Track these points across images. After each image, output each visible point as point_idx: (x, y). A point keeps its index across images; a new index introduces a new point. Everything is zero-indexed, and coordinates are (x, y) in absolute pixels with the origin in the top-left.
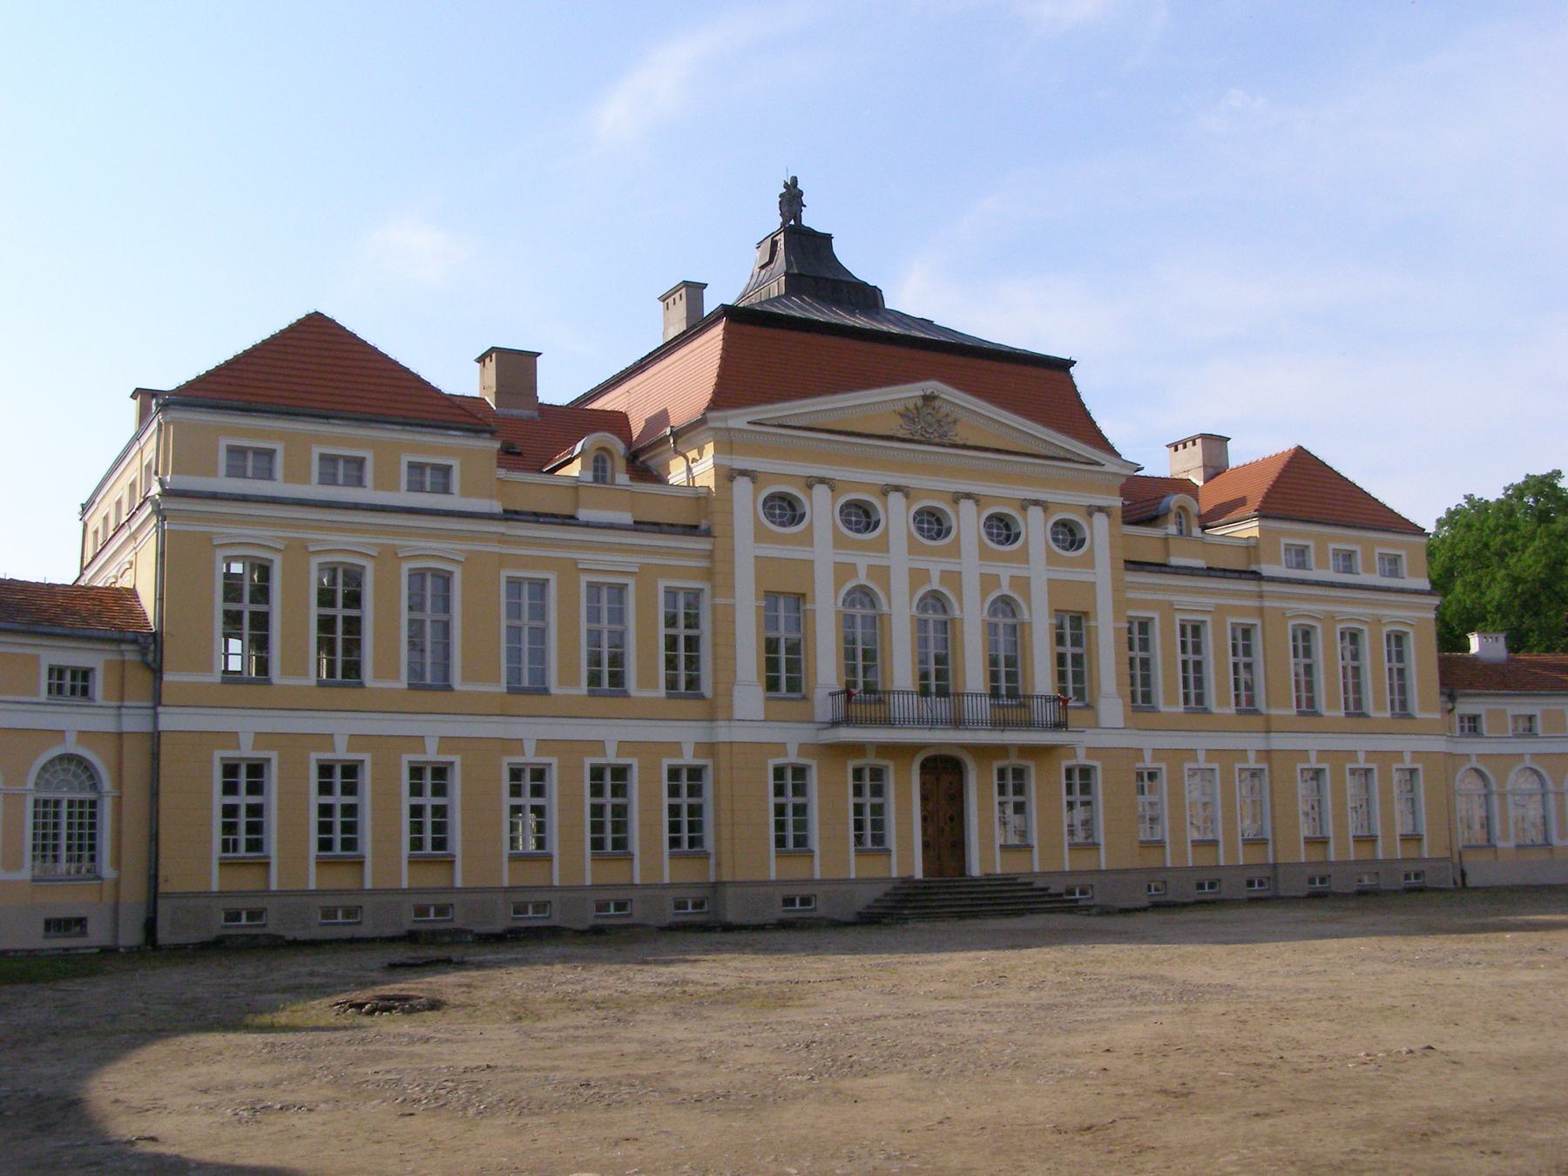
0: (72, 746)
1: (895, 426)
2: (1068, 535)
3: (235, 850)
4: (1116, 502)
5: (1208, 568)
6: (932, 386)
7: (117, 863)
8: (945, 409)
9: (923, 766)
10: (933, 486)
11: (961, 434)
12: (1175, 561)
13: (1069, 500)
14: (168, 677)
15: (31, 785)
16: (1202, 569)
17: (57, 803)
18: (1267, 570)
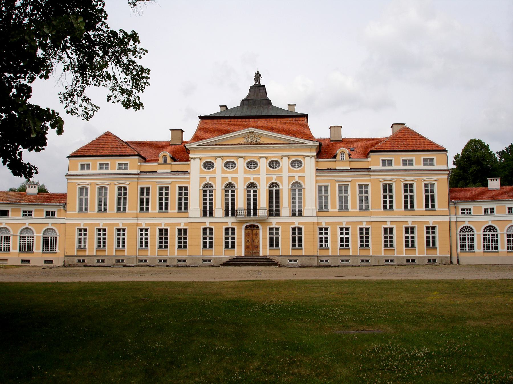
0: (50, 226)
1: (241, 141)
2: (296, 164)
3: (81, 247)
4: (315, 153)
5: (351, 169)
6: (251, 129)
7: (59, 249)
8: (257, 135)
9: (246, 227)
10: (252, 155)
11: (263, 140)
12: (337, 168)
13: (296, 154)
14: (67, 212)
15: (42, 234)
16: (349, 169)
17: (48, 238)
18: (373, 168)
